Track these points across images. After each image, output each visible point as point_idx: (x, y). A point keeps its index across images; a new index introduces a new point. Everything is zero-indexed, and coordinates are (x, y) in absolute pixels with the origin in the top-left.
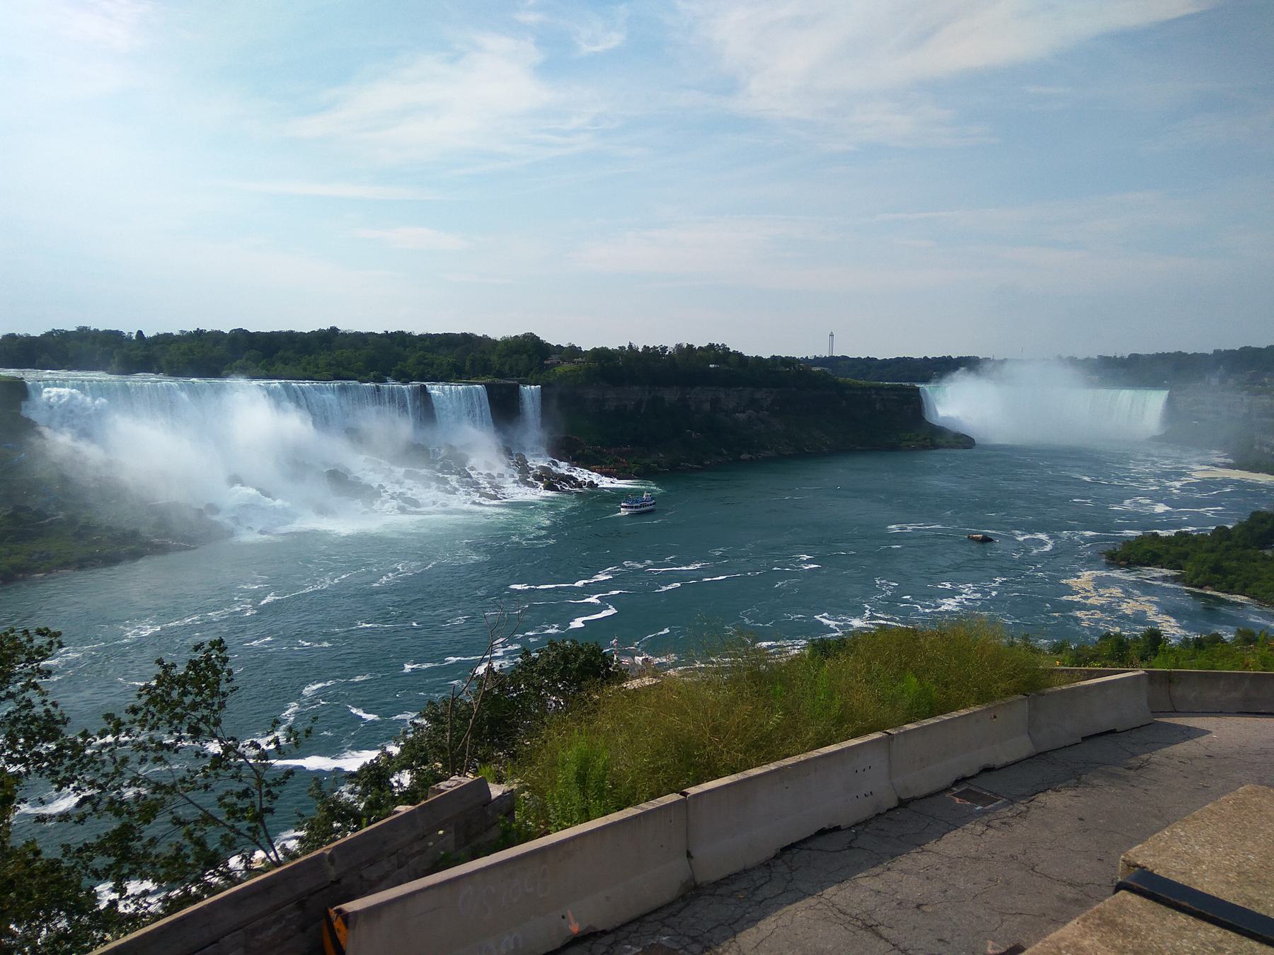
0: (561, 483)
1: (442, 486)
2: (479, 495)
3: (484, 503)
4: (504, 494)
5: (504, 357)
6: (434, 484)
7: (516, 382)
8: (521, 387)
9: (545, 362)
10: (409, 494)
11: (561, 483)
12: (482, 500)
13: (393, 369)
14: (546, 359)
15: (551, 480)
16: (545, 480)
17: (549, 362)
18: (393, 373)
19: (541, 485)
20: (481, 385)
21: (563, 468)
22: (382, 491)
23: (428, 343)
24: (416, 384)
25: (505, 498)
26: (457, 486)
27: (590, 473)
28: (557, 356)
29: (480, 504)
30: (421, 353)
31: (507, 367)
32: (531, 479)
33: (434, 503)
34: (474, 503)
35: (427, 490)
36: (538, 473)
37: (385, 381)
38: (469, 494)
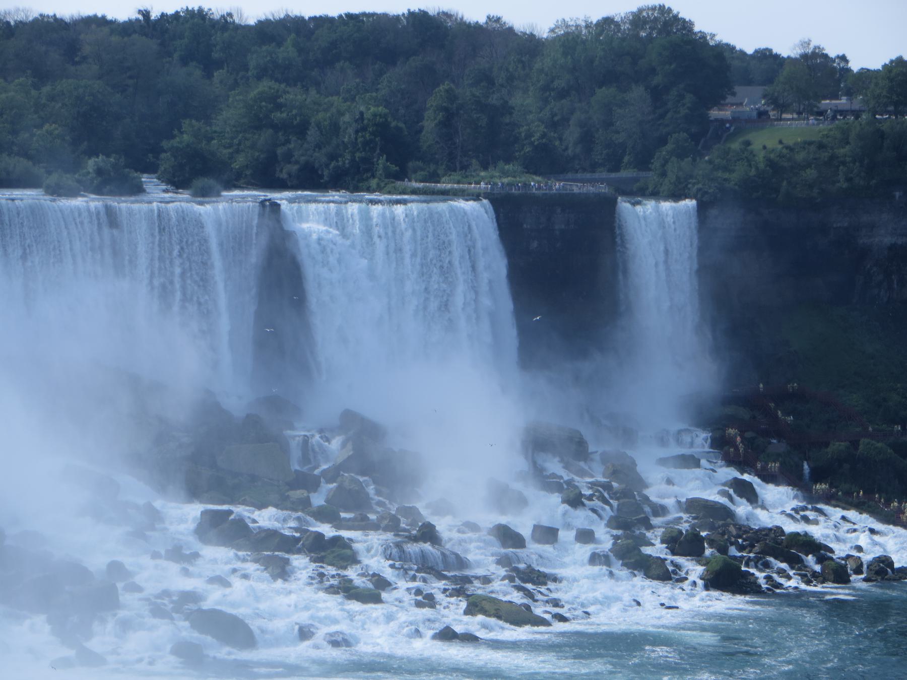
0: (767, 565)
1: (331, 570)
2: (464, 605)
3: (482, 634)
4: (556, 603)
5: (563, 94)
6: (301, 563)
7: (603, 189)
8: (624, 205)
9: (715, 113)
10: (214, 598)
11: (767, 565)
12: (474, 624)
13: (165, 144)
14: (717, 100)
15: (733, 551)
16: (708, 552)
17: (726, 113)
18: (166, 161)
19: (694, 570)
20: (476, 197)
22: (120, 585)
23: (287, 51)
25: (562, 619)
26: (388, 574)
27: (878, 526)
28: (759, 90)
29: (469, 638)
30: (266, 85)
31: (572, 134)
32: (657, 549)
33: (305, 633)
34: (447, 635)
35: (279, 583)
36: (684, 527)
37: (137, 190)
38: (429, 601)
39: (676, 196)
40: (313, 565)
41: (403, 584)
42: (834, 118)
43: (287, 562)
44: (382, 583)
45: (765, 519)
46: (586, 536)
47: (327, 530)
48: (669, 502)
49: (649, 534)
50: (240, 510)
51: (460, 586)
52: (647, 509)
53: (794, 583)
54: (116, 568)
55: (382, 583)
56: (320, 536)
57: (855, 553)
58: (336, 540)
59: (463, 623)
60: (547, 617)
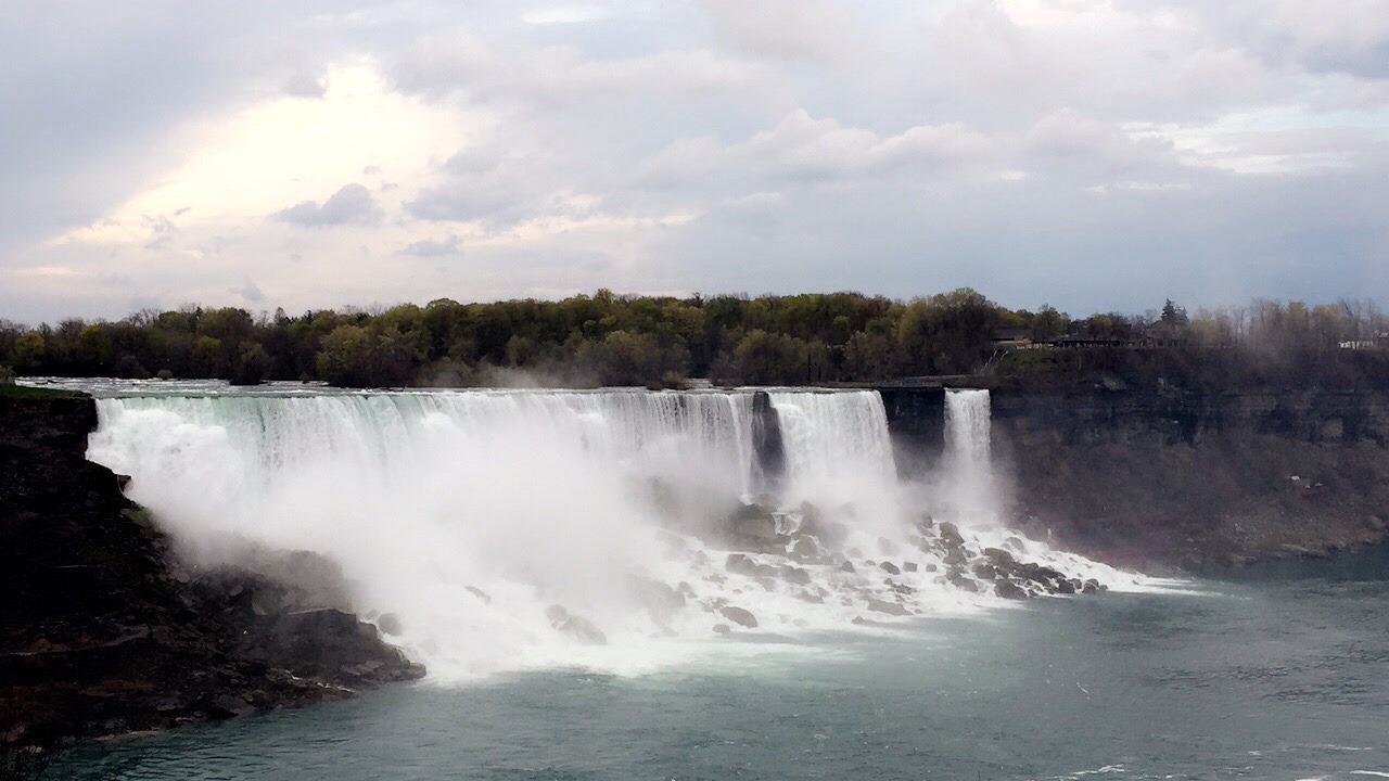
0: (1029, 584)
4: (916, 604)
6: (781, 584)
11: (1029, 584)
12: (875, 616)
15: (1011, 576)
20: (872, 389)
21: (1035, 552)
22: (686, 594)
24: (748, 392)
29: (870, 623)
32: (970, 575)
34: (859, 621)
36: (985, 564)
39: (978, 388)
40: (788, 584)
41: (835, 594)
42: (1062, 346)
43: (773, 581)
44: (823, 593)
45: (1027, 559)
46: (932, 568)
47: (794, 564)
48: (976, 550)
49: (965, 567)
50: (749, 555)
51: (866, 595)
52: (965, 554)
53: (1045, 593)
54: (684, 586)
55: (823, 593)
56: (791, 568)
57: (1077, 578)
58: (800, 570)
59: (867, 614)
60: (912, 611)
